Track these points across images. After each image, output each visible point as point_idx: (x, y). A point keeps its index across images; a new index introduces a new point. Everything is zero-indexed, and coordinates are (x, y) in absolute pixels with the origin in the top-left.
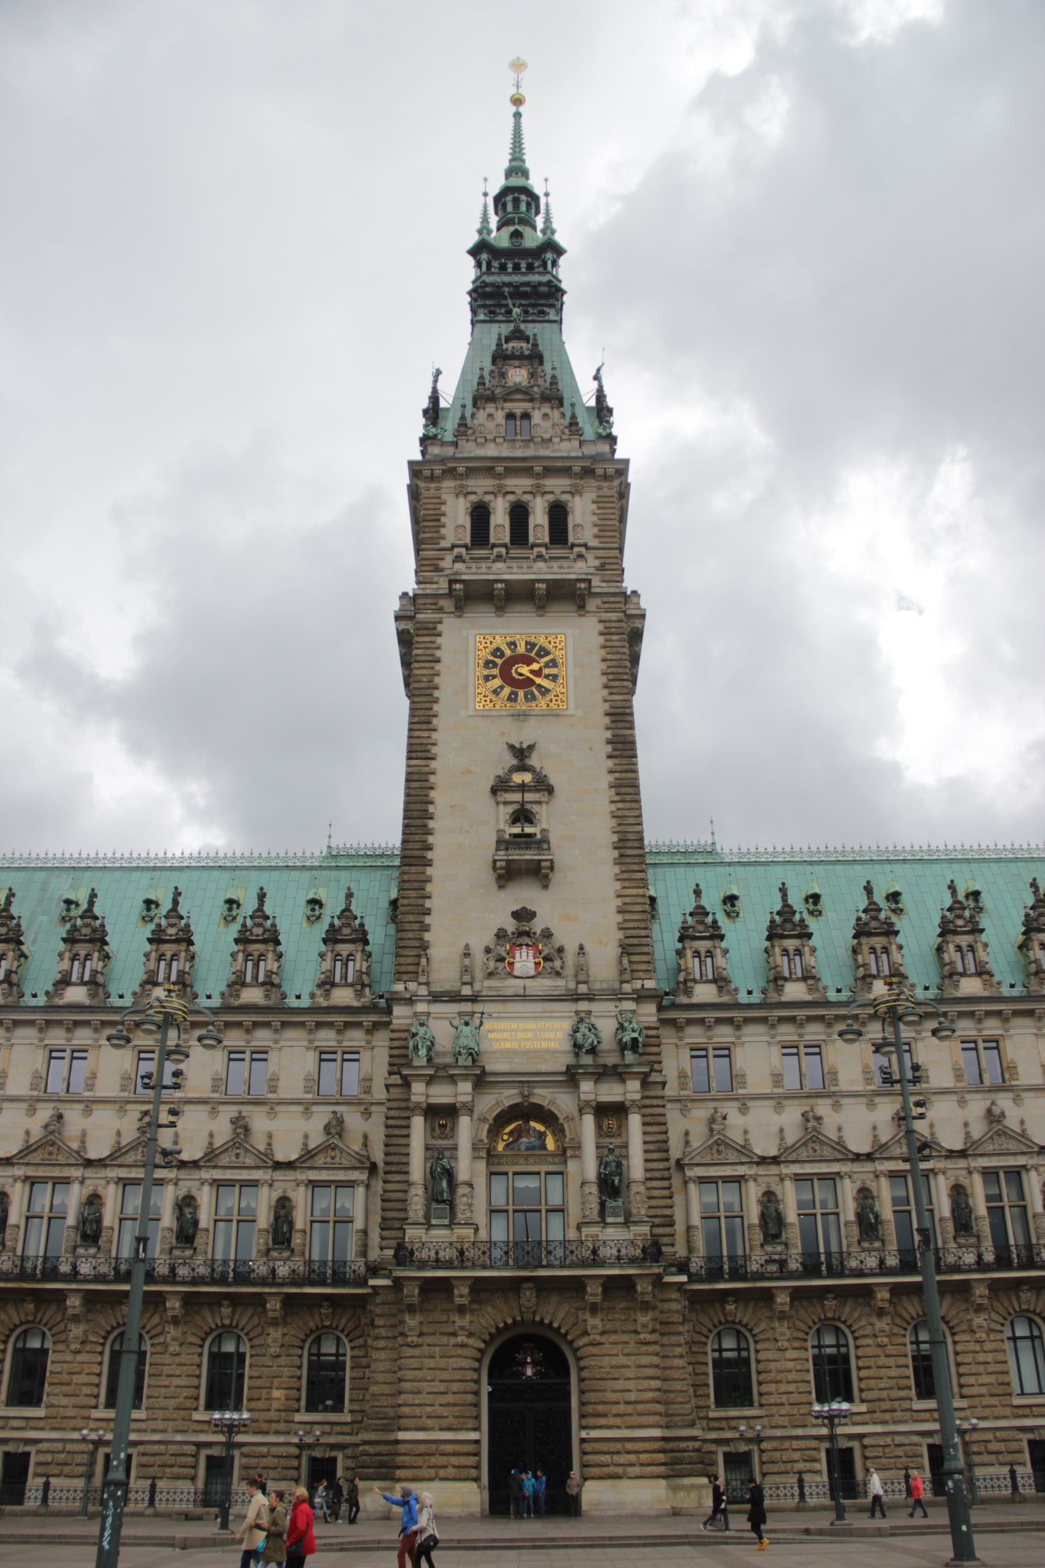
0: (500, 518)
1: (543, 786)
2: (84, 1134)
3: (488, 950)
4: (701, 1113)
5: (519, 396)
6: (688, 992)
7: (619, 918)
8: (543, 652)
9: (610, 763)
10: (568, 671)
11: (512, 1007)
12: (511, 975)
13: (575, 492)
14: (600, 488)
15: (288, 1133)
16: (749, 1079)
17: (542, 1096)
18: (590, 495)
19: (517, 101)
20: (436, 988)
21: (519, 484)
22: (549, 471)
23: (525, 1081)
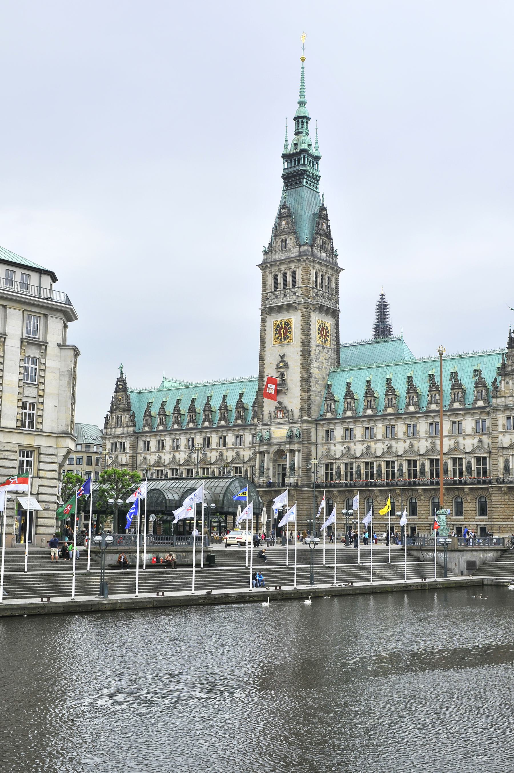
0: (280, 280)
1: (286, 366)
2: (210, 457)
3: (274, 412)
4: (326, 447)
5: (284, 233)
6: (326, 415)
7: (300, 401)
8: (288, 324)
9: (301, 358)
10: (294, 330)
11: (278, 426)
12: (278, 418)
13: (298, 268)
14: (303, 265)
15: (246, 454)
16: (337, 438)
17: (282, 448)
18: (301, 268)
19: (303, 60)
20: (264, 422)
21: (283, 267)
22: (290, 262)
23: (279, 444)
